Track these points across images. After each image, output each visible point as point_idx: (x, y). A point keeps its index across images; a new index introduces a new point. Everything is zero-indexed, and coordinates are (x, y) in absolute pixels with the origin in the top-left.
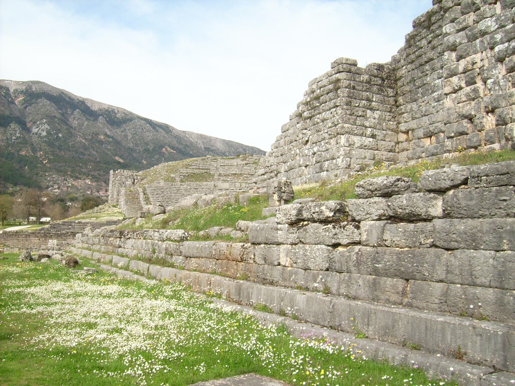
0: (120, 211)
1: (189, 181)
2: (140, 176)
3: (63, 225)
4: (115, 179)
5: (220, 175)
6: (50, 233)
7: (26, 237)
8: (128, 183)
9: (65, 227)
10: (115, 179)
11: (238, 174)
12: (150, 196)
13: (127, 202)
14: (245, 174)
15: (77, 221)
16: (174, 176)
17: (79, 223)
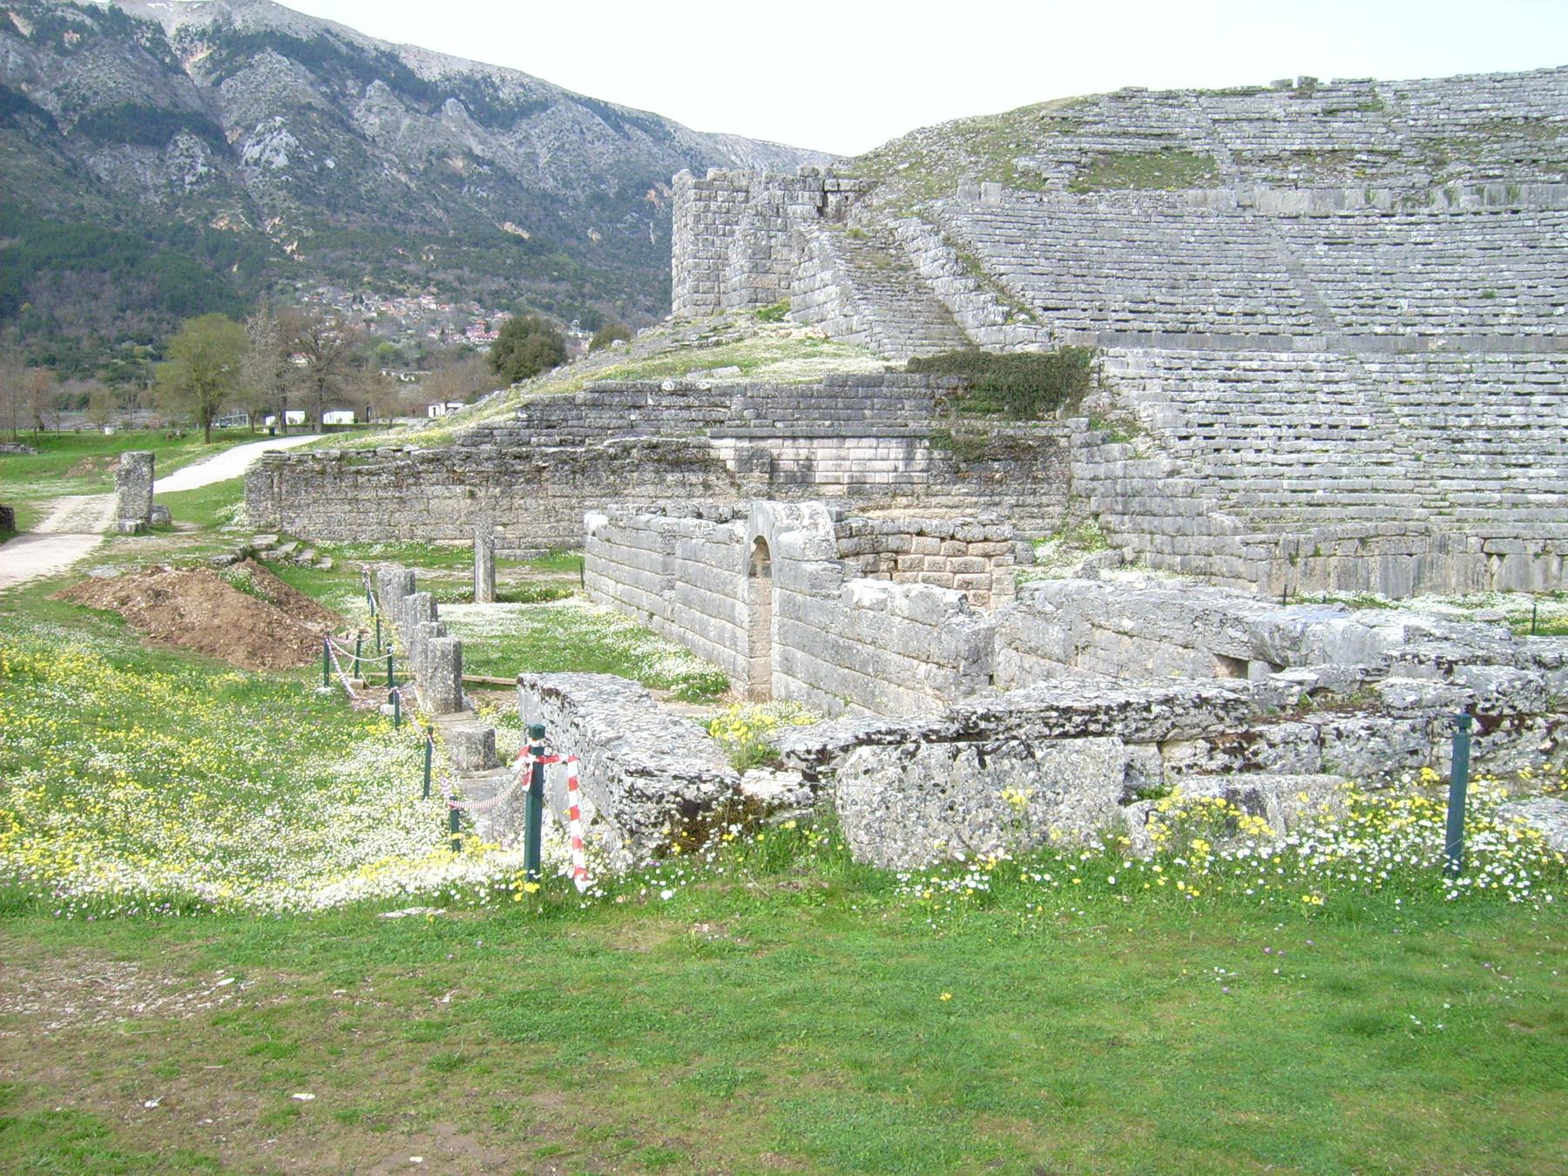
0: (817, 331)
1: (1108, 187)
2: (849, 178)
3: (595, 405)
4: (707, 209)
5: (1237, 157)
6: (527, 457)
7: (398, 486)
8: (799, 209)
9: (608, 418)
10: (707, 209)
11: (1321, 153)
12: (984, 250)
13: (862, 287)
14: (1352, 151)
15: (668, 385)
16: (1032, 164)
17: (683, 391)
